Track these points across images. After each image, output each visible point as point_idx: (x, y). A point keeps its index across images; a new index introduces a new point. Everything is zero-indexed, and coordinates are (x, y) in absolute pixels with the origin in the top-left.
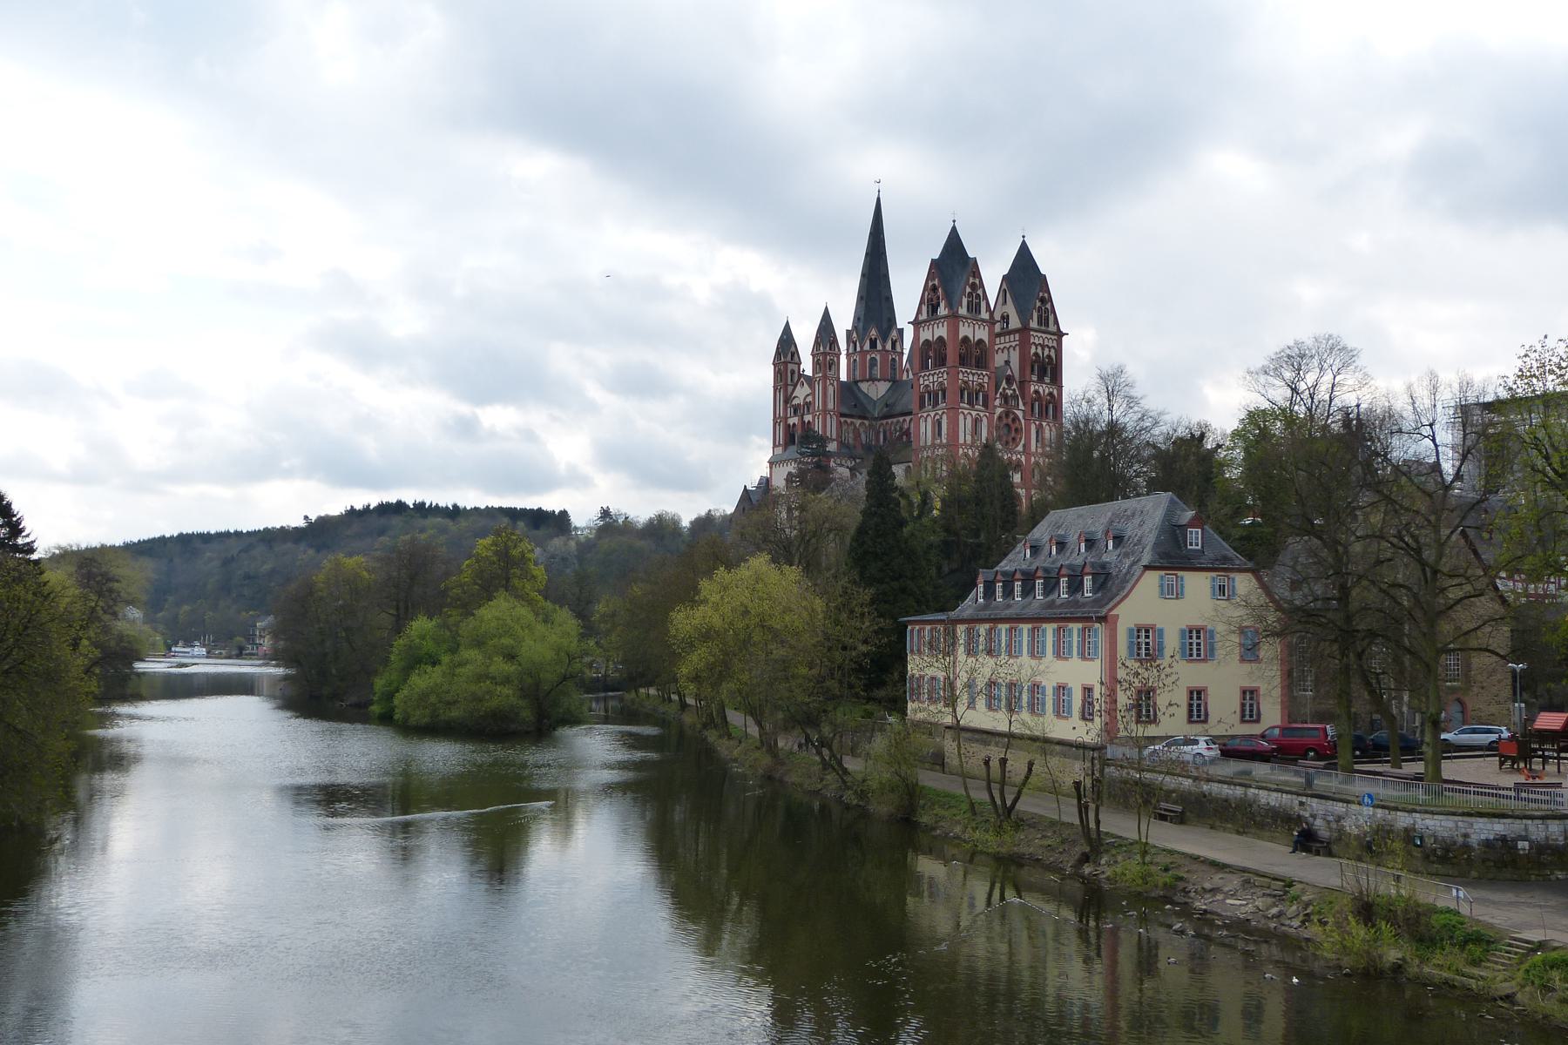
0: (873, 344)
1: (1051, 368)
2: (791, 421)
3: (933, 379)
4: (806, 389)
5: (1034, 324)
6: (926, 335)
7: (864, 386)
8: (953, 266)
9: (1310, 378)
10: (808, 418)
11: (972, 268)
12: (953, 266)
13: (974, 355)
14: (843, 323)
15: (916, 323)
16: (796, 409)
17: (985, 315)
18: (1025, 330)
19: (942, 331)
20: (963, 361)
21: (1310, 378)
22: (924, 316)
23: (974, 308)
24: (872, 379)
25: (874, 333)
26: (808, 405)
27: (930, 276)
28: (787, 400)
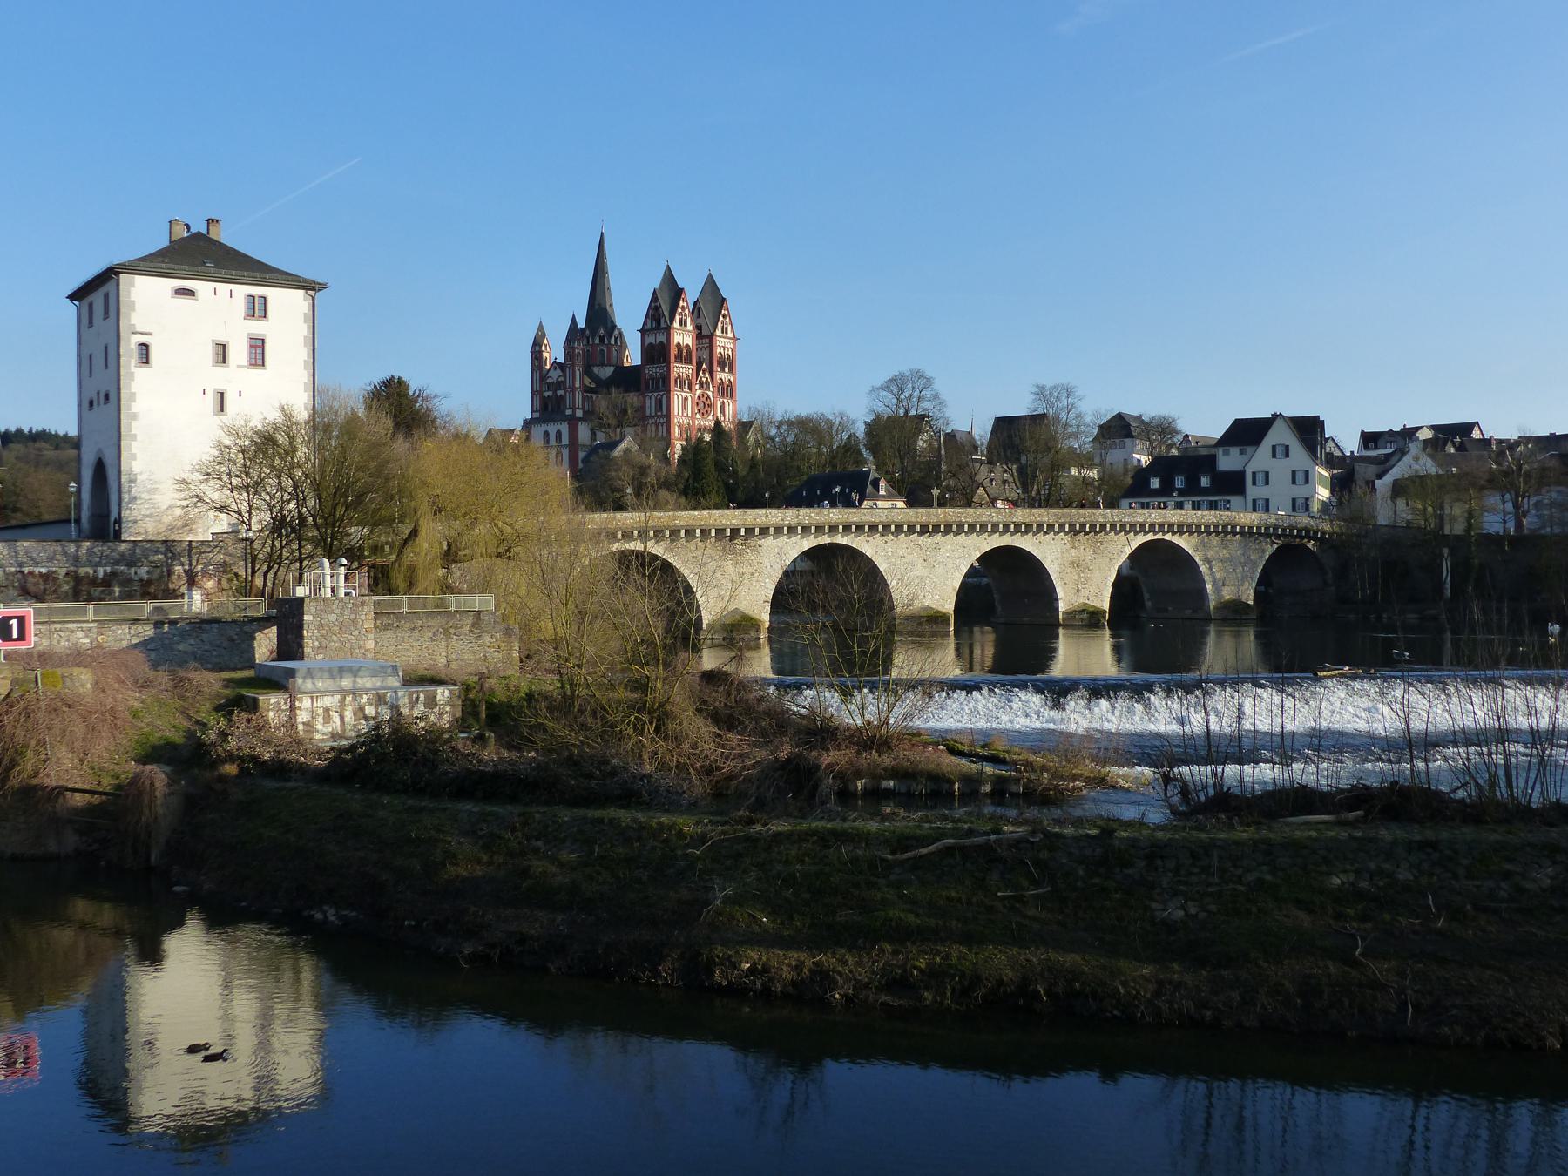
0: (602, 339)
1: (728, 363)
2: (546, 394)
3: (652, 371)
4: (559, 372)
5: (718, 332)
6: (650, 339)
7: (596, 370)
8: (671, 289)
9: (907, 394)
10: (560, 393)
11: (677, 293)
12: (671, 289)
13: (684, 356)
14: (581, 323)
15: (643, 331)
16: (550, 386)
17: (690, 327)
18: (711, 337)
19: (662, 338)
20: (679, 358)
21: (907, 394)
22: (648, 326)
23: (683, 323)
24: (602, 365)
25: (602, 331)
26: (560, 383)
27: (654, 298)
28: (543, 378)
